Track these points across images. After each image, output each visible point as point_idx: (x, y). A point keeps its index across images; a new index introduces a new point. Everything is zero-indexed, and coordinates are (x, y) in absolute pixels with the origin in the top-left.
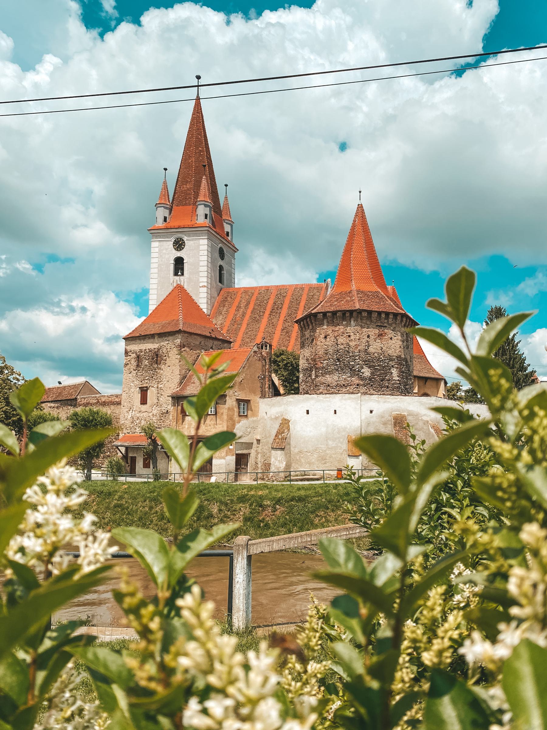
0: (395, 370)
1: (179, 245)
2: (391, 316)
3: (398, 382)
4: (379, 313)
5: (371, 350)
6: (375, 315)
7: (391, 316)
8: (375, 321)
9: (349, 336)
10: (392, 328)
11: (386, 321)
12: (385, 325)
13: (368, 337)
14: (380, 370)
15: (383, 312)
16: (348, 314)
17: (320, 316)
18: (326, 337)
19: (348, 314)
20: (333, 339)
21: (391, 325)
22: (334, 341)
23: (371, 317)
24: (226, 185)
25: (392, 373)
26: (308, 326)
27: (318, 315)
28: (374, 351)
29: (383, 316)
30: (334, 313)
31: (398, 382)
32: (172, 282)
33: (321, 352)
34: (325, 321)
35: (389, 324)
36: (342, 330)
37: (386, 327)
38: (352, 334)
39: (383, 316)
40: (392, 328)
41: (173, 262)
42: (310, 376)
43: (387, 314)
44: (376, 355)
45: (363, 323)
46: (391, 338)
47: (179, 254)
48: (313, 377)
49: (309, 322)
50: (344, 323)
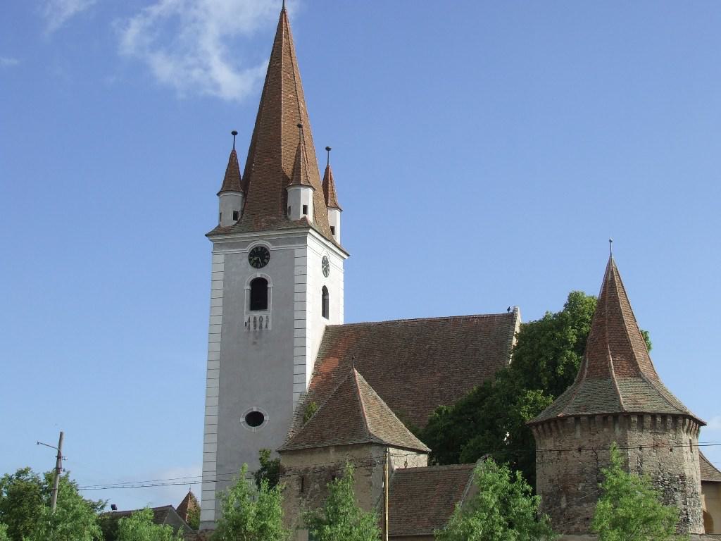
0: (679, 494)
1: (259, 257)
2: (669, 420)
4: (654, 416)
7: (669, 420)
10: (671, 435)
15: (658, 414)
16: (610, 419)
17: (571, 421)
18: (580, 450)
19: (610, 419)
22: (592, 456)
24: (328, 149)
26: (551, 431)
27: (569, 419)
29: (659, 419)
30: (591, 417)
31: (685, 512)
32: (246, 320)
33: (574, 472)
34: (578, 428)
36: (602, 441)
39: (659, 419)
40: (671, 435)
41: (249, 287)
42: (558, 504)
43: (664, 416)
45: (633, 431)
46: (671, 450)
47: (259, 274)
48: (564, 505)
49: (553, 428)
50: (605, 430)
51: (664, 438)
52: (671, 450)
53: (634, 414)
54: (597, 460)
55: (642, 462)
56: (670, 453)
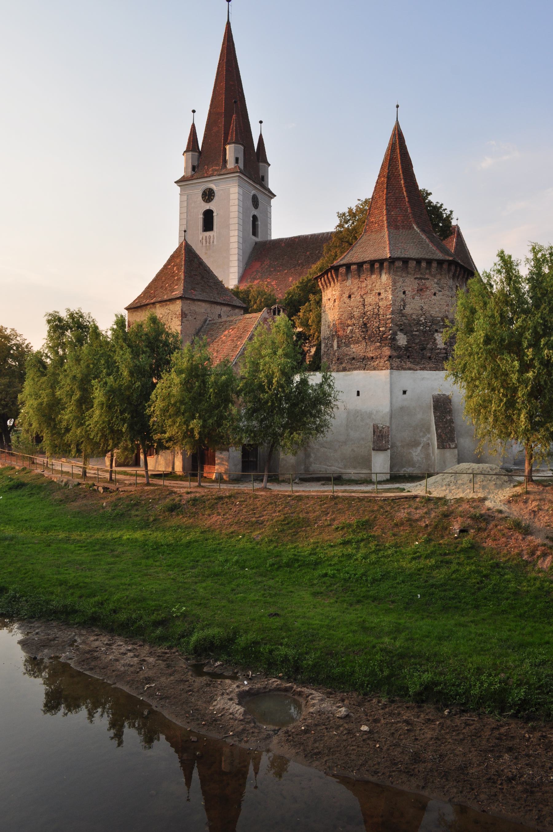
2: (434, 265)
3: (444, 351)
4: (418, 261)
5: (408, 310)
6: (412, 264)
7: (434, 265)
8: (413, 272)
9: (379, 294)
10: (436, 280)
11: (428, 271)
12: (427, 276)
13: (404, 293)
14: (418, 336)
15: (424, 259)
19: (377, 265)
20: (358, 298)
21: (434, 276)
23: (407, 267)
25: (435, 340)
28: (411, 312)
29: (424, 264)
31: (444, 351)
35: (432, 276)
36: (369, 287)
37: (428, 279)
38: (382, 291)
39: (424, 264)
40: (436, 280)
44: (414, 317)
46: (435, 294)
51: (428, 283)
52: (435, 294)
53: (398, 259)
54: (364, 305)
55: (404, 306)
56: (433, 297)
